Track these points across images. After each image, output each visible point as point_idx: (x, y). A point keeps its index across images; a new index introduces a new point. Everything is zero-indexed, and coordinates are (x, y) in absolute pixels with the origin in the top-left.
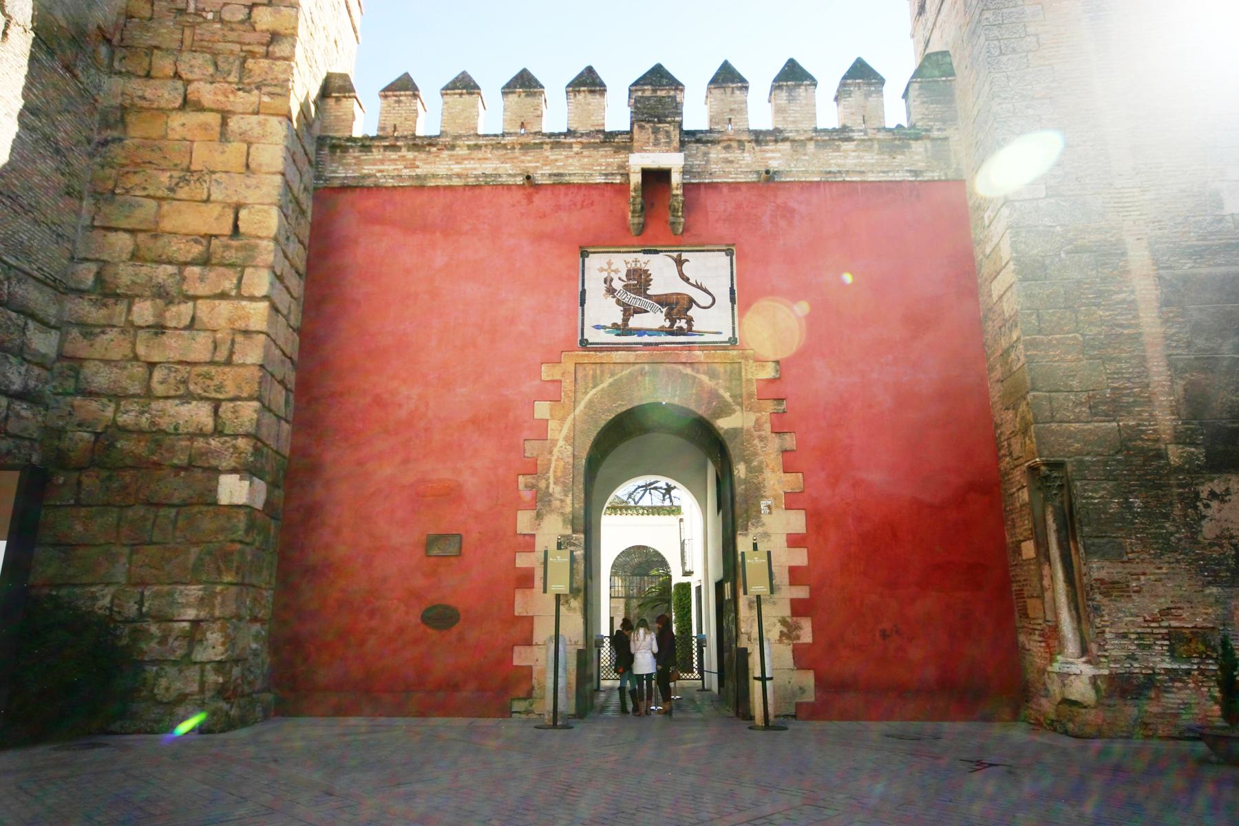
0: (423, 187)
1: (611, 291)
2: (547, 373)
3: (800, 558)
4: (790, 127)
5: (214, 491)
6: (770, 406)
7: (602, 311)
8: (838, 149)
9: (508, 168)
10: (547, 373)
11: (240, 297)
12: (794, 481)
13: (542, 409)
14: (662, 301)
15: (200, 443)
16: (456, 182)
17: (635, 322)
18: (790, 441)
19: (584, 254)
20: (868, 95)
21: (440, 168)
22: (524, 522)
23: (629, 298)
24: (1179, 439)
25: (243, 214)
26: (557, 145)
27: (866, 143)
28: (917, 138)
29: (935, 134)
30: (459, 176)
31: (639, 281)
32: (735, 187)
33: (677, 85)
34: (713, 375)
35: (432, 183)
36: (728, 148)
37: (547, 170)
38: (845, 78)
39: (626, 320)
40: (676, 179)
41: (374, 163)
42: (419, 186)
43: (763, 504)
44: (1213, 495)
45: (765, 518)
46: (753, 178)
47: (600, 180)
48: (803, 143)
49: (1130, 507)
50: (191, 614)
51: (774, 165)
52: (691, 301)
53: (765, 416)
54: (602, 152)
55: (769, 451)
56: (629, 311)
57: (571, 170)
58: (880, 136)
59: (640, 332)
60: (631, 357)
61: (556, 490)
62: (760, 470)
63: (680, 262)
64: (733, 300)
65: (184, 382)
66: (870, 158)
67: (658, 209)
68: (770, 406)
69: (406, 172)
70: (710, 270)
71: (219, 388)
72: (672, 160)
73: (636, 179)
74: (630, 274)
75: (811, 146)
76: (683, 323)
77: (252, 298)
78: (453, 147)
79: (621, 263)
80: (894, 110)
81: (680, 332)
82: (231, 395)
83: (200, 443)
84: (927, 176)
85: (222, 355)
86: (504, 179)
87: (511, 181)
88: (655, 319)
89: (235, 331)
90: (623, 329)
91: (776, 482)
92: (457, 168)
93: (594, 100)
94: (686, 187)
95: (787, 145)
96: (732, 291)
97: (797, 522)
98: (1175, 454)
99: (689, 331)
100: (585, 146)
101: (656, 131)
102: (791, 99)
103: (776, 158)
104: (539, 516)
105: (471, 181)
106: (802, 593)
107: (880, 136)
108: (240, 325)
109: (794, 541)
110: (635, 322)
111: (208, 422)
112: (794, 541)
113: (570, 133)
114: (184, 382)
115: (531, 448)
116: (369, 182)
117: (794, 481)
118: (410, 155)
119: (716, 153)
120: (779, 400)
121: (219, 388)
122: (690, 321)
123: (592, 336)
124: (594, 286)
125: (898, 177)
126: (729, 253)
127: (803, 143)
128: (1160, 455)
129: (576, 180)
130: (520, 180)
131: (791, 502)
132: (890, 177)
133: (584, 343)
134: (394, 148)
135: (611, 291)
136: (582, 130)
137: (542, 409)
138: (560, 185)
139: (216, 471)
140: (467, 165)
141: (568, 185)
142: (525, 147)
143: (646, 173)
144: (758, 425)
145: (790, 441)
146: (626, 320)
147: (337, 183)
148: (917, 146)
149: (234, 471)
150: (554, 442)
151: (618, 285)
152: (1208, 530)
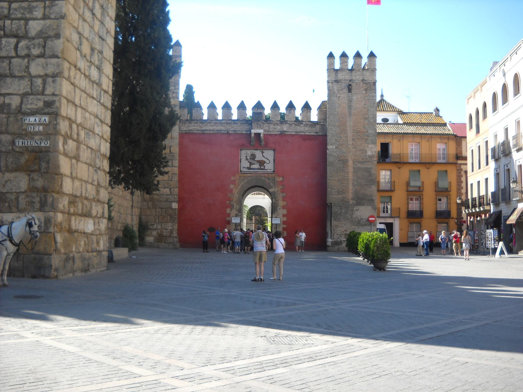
0: (203, 134)
1: (247, 159)
2: (233, 178)
3: (285, 219)
4: (289, 120)
5: (171, 206)
6: (281, 187)
7: (245, 164)
8: (300, 126)
9: (223, 128)
10: (233, 178)
11: (172, 166)
12: (284, 203)
13: (232, 186)
14: (259, 162)
15: (168, 197)
16: (211, 132)
17: (252, 166)
18: (284, 195)
19: (241, 150)
20: (307, 113)
21: (209, 127)
22: (228, 211)
23: (251, 161)
24: (353, 199)
25: (171, 148)
26: (235, 123)
27: (306, 125)
28: (318, 124)
29: (322, 123)
30: (212, 130)
31: (253, 156)
32: (275, 135)
33: (263, 108)
34: (269, 179)
35: (206, 132)
36: (274, 125)
37: (232, 129)
38: (302, 108)
39: (250, 166)
40: (262, 135)
41: (192, 126)
42: (203, 133)
43: (278, 208)
44: (356, 210)
45: (278, 211)
46: (279, 133)
47: (245, 132)
48: (292, 124)
49: (342, 211)
50: (170, 228)
51: (285, 129)
52: (265, 162)
53: (279, 189)
54: (245, 125)
55: (280, 196)
56: (251, 164)
57: (238, 129)
58: (309, 123)
59: (253, 169)
60: (251, 175)
61: (235, 204)
62: (278, 201)
63: (263, 153)
64: (274, 162)
65: (164, 184)
66: (307, 129)
67: (258, 142)
68: (281, 187)
69: (200, 129)
70: (269, 154)
71: (170, 186)
72: (261, 131)
73: (253, 135)
74: (251, 155)
75: (294, 125)
76: (263, 167)
77: (175, 167)
78: (210, 123)
79: (249, 152)
80: (314, 117)
81: (262, 169)
82: (173, 187)
83: (168, 197)
84: (319, 134)
85: (170, 179)
86: (222, 132)
87: (224, 132)
88: (256, 166)
89: (173, 174)
90: (249, 168)
91: (281, 203)
92: (211, 128)
93: (243, 111)
94: (264, 135)
95: (288, 125)
96: (274, 160)
97: (285, 212)
98: (351, 202)
99: (264, 169)
100: (241, 123)
101: (257, 124)
102: (290, 113)
103: (285, 128)
104: (231, 209)
105: (215, 132)
106: (285, 226)
107: (309, 123)
108: (173, 172)
109: (284, 216)
110: (252, 166)
111: (169, 192)
112: (284, 216)
113: (238, 120)
114: (164, 184)
115: (229, 195)
116: (192, 132)
117: (284, 203)
118: (200, 125)
119: (272, 126)
120: (283, 185)
121: (170, 186)
122: (264, 167)
123: (243, 170)
124: (243, 158)
125: (312, 134)
126: (274, 150)
127: (292, 124)
128: (349, 202)
129: (239, 132)
130: (226, 132)
131: (284, 207)
132: (311, 134)
133: (241, 171)
134: (197, 123)
135: (247, 159)
136: (241, 119)
137: (232, 186)
138: (236, 134)
139: (171, 202)
140: (214, 127)
141: (238, 133)
142: (228, 123)
143: (255, 133)
144: (278, 191)
145: (284, 195)
146: (250, 166)
147: (184, 132)
148: (318, 126)
149: (174, 202)
150: (234, 194)
151: (248, 158)
152: (354, 216)
